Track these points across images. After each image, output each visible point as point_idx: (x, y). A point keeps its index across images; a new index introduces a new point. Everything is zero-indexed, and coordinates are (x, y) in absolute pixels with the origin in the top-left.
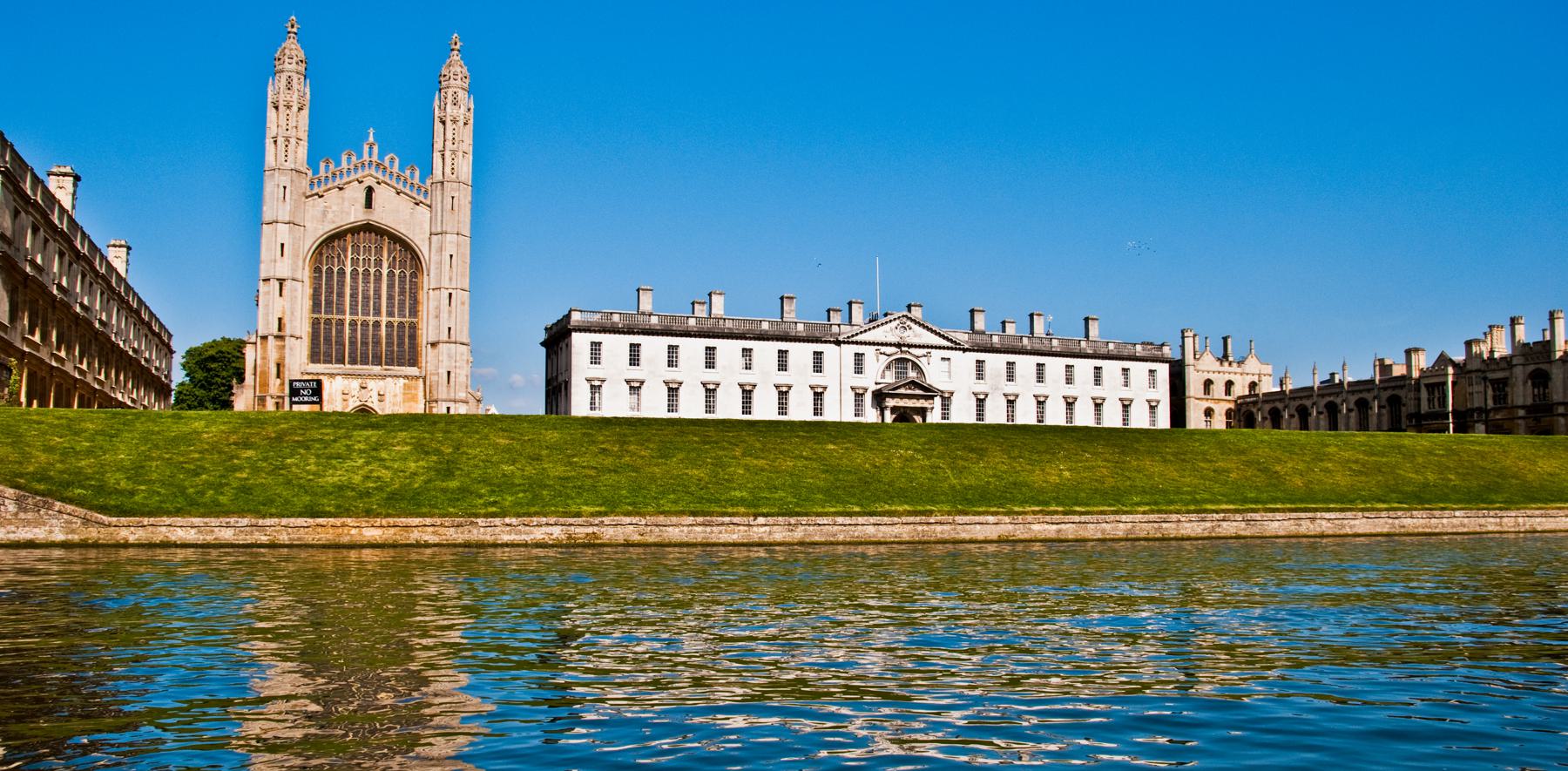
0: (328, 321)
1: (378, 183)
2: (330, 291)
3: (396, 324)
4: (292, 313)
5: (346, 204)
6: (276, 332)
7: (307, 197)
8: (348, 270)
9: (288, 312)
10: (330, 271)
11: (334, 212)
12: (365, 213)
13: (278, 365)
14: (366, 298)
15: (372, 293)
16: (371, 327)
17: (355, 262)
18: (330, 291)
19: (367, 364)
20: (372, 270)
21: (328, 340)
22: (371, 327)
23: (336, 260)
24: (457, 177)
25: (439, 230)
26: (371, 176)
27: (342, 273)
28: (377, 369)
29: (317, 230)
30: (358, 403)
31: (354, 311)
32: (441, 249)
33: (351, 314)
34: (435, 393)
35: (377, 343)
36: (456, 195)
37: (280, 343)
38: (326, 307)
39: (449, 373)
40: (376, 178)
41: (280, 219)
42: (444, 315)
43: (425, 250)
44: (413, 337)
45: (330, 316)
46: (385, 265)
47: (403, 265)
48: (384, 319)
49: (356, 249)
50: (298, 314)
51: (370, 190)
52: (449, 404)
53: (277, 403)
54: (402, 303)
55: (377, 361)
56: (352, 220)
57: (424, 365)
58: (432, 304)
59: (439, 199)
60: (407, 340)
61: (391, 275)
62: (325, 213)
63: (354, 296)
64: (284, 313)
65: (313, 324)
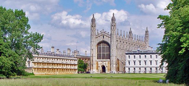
8: (101, 47)
10: (99, 47)
17: (102, 46)
27: (101, 47)
28: (105, 60)
31: (102, 52)
42: (112, 52)
44: (110, 55)
48: (106, 53)
51: (103, 36)
54: (108, 51)
55: (105, 59)
61: (107, 47)
62: (98, 40)
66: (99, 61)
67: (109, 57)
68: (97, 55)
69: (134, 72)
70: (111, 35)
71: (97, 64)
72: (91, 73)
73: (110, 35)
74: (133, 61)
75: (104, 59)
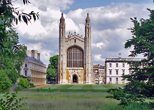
2: (69, 56)
18: (69, 56)
20: (76, 52)
21: (69, 64)
27: (71, 53)
28: (77, 68)
30: (74, 74)
31: (73, 59)
33: (73, 59)
39: (88, 69)
44: (83, 63)
47: (81, 51)
51: (75, 40)
54: (81, 57)
62: (68, 44)
63: (73, 57)
66: (70, 69)
67: (83, 64)
68: (66, 62)
69: (117, 83)
70: (85, 38)
71: (68, 73)
72: (61, 83)
74: (116, 70)
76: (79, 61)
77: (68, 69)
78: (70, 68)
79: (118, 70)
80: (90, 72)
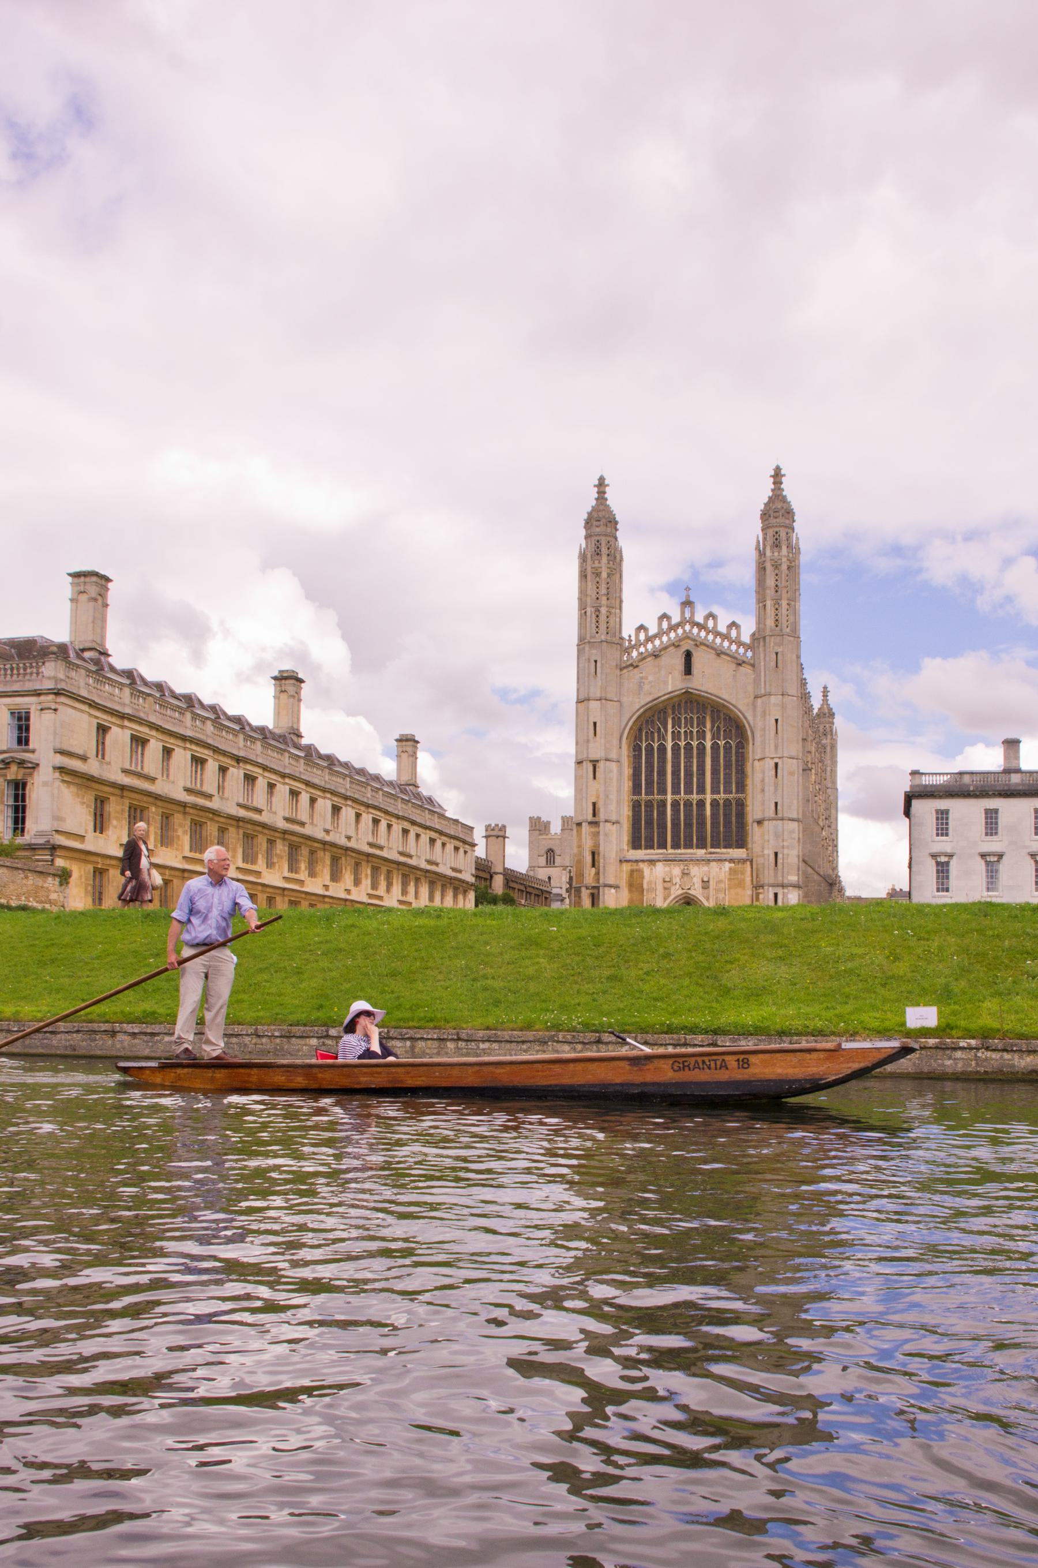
0: (649, 804)
1: (696, 645)
3: (721, 802)
4: (607, 796)
5: (663, 673)
6: (590, 818)
7: (621, 669)
8: (669, 745)
9: (602, 796)
10: (650, 749)
11: (650, 682)
12: (683, 680)
13: (593, 854)
14: (689, 774)
15: (695, 768)
16: (695, 806)
17: (676, 736)
19: (691, 847)
20: (695, 743)
21: (649, 823)
22: (695, 806)
23: (656, 735)
24: (781, 630)
25: (763, 692)
26: (688, 638)
27: (662, 749)
28: (701, 852)
29: (635, 703)
30: (680, 892)
31: (676, 791)
32: (764, 713)
33: (673, 793)
34: (761, 876)
35: (702, 823)
36: (779, 650)
37: (593, 830)
38: (646, 788)
39: (776, 854)
40: (694, 640)
41: (592, 695)
42: (770, 789)
43: (750, 718)
44: (741, 815)
45: (650, 797)
46: (709, 736)
48: (708, 797)
49: (677, 723)
50: (613, 797)
51: (688, 655)
52: (776, 890)
53: (593, 895)
54: (727, 776)
55: (702, 845)
56: (670, 689)
57: (750, 846)
58: (758, 776)
59: (762, 656)
60: (734, 819)
61: (715, 747)
62: (640, 687)
64: (598, 797)
65: (634, 807)
68: (626, 812)
73: (748, 647)
74: (983, 856)
75: (689, 845)
76: (715, 804)
77: (637, 861)
78: (655, 853)
79: (1000, 856)
80: (793, 878)
